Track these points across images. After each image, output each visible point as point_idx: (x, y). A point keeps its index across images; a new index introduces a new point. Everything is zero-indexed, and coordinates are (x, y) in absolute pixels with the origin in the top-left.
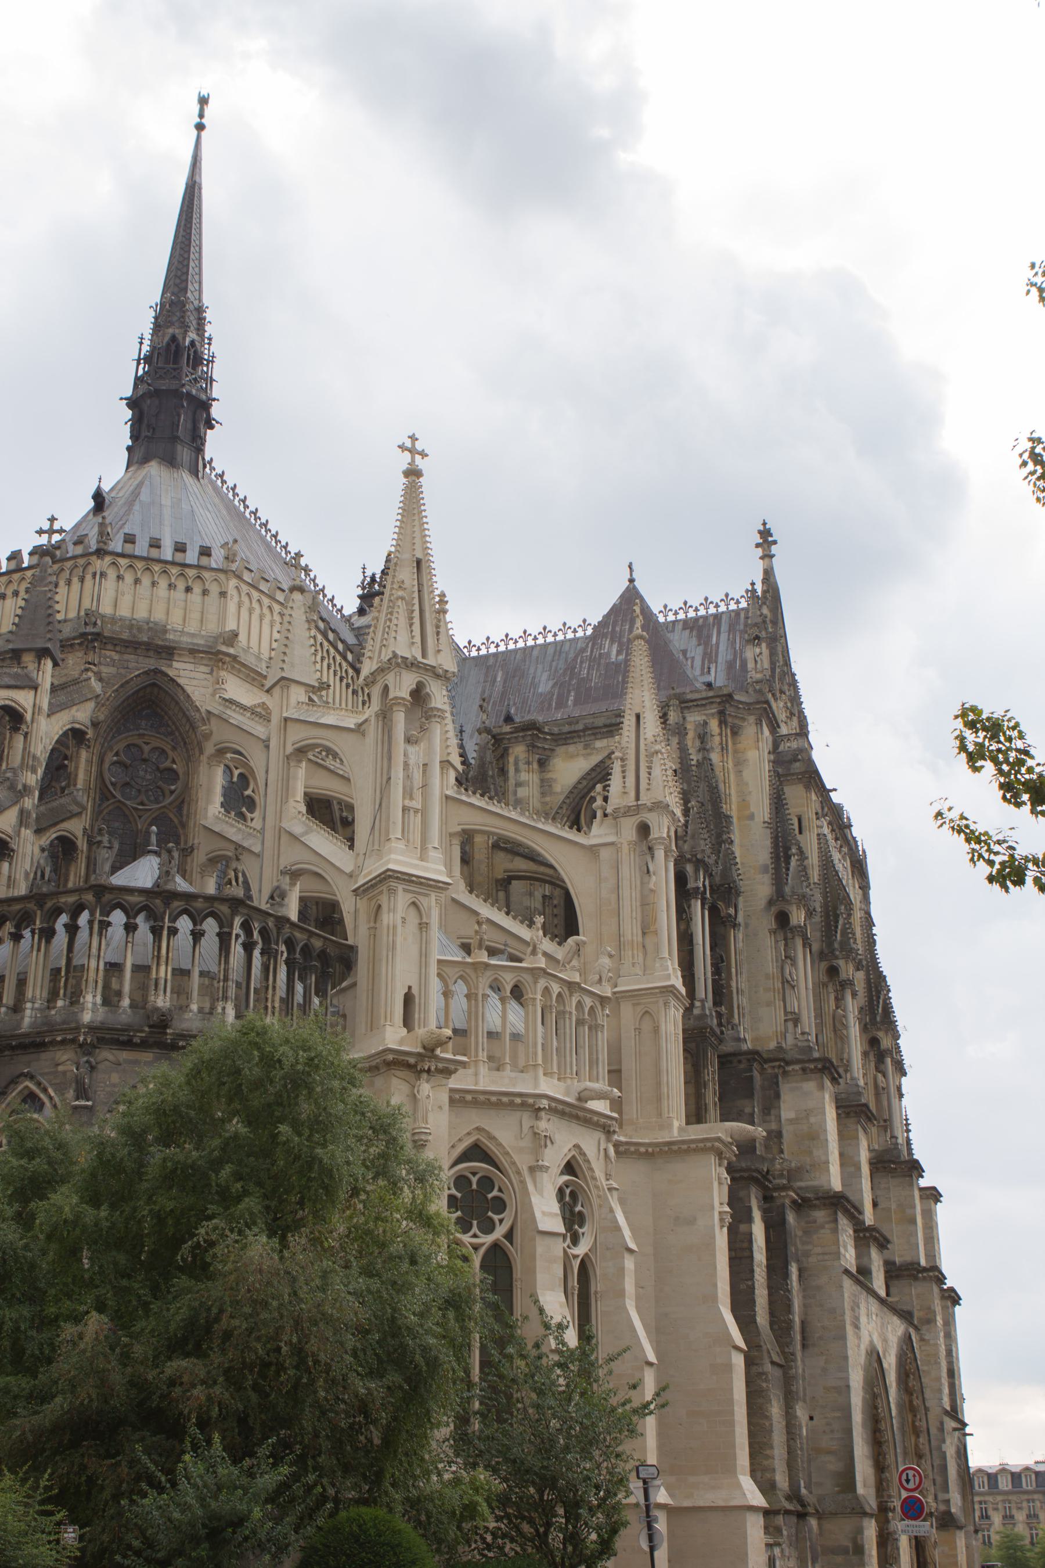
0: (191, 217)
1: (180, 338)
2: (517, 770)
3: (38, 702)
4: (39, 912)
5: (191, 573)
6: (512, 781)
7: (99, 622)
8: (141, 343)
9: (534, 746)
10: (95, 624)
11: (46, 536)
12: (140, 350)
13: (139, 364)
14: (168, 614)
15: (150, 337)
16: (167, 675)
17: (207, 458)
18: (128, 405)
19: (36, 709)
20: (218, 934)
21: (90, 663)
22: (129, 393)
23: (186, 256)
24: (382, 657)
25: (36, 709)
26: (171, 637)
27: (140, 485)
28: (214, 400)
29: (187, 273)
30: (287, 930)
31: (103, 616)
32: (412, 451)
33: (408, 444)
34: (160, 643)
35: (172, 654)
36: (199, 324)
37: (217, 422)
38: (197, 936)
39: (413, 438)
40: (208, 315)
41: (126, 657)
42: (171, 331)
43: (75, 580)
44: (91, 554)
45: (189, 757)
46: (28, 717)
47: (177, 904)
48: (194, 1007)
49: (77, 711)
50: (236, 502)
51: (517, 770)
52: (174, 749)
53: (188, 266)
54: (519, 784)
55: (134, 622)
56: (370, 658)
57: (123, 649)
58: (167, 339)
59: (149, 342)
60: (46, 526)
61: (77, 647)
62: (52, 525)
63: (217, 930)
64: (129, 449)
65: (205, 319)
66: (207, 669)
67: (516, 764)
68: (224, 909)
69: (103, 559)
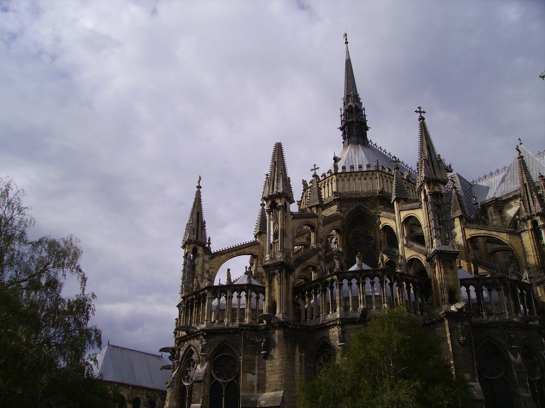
2: (492, 216)
3: (319, 221)
4: (320, 284)
6: (490, 220)
8: (341, 110)
9: (496, 206)
11: (314, 171)
12: (341, 112)
13: (341, 117)
17: (369, 140)
19: (319, 224)
20: (379, 282)
24: (421, 180)
25: (319, 224)
30: (404, 277)
32: (420, 112)
33: (418, 110)
36: (357, 100)
37: (369, 128)
38: (372, 284)
39: (420, 108)
40: (360, 96)
41: (349, 204)
43: (330, 184)
44: (333, 175)
45: (375, 231)
46: (316, 227)
47: (364, 274)
48: (374, 307)
49: (335, 223)
50: (382, 152)
51: (492, 216)
52: (370, 230)
54: (493, 220)
56: (418, 182)
57: (348, 202)
60: (313, 168)
62: (315, 167)
63: (379, 280)
65: (359, 98)
67: (491, 214)
68: (380, 273)
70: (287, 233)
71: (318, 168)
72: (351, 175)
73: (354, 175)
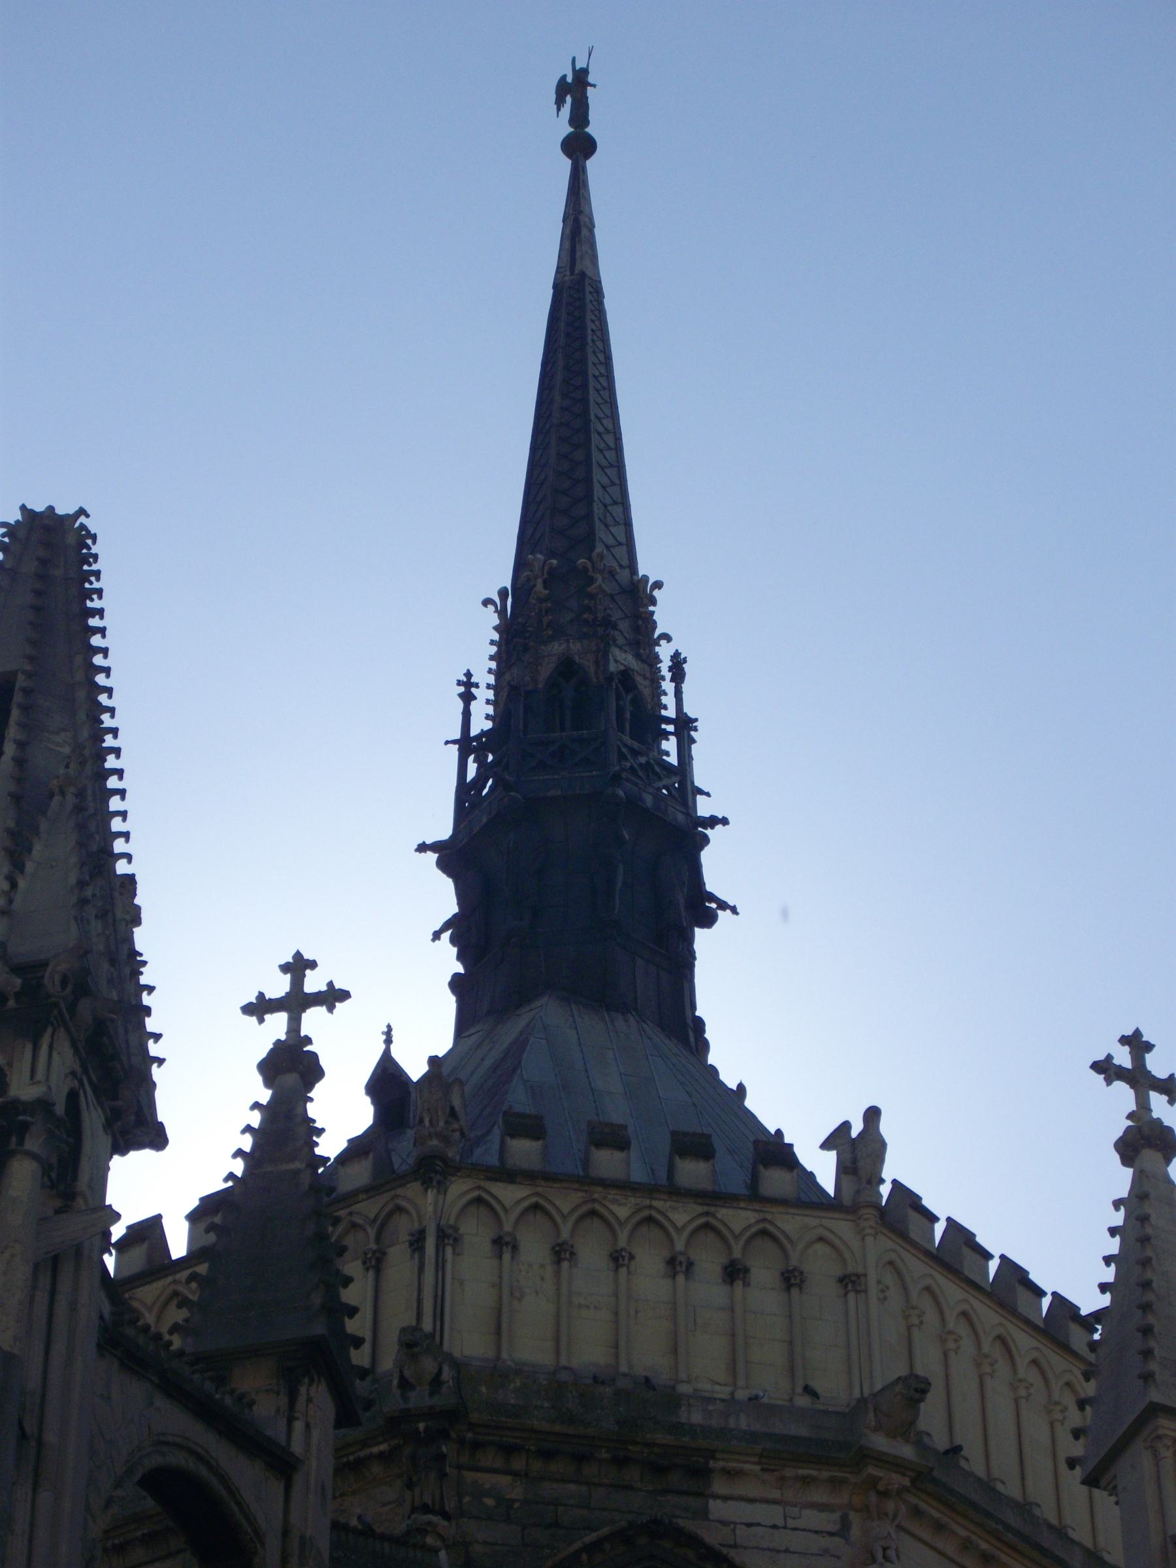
0: (583, 361)
1: (588, 664)
5: (739, 1219)
7: (447, 1374)
8: (467, 698)
10: (436, 1382)
12: (467, 715)
14: (675, 1350)
15: (491, 679)
16: (693, 1541)
18: (443, 865)
21: (426, 1509)
22: (443, 828)
23: (579, 455)
26: (697, 1418)
27: (520, 1044)
28: (713, 821)
29: (589, 497)
31: (458, 1366)
34: (661, 1438)
35: (702, 1473)
37: (723, 905)
42: (557, 648)
44: (402, 1179)
53: (588, 480)
55: (563, 1376)
57: (537, 1465)
58: (546, 670)
59: (490, 695)
60: (278, 987)
61: (376, 1469)
64: (456, 984)
66: (828, 1521)
69: (442, 1188)
70: (51, 1437)
71: (333, 997)
72: (593, 1213)
73: (622, 1212)
